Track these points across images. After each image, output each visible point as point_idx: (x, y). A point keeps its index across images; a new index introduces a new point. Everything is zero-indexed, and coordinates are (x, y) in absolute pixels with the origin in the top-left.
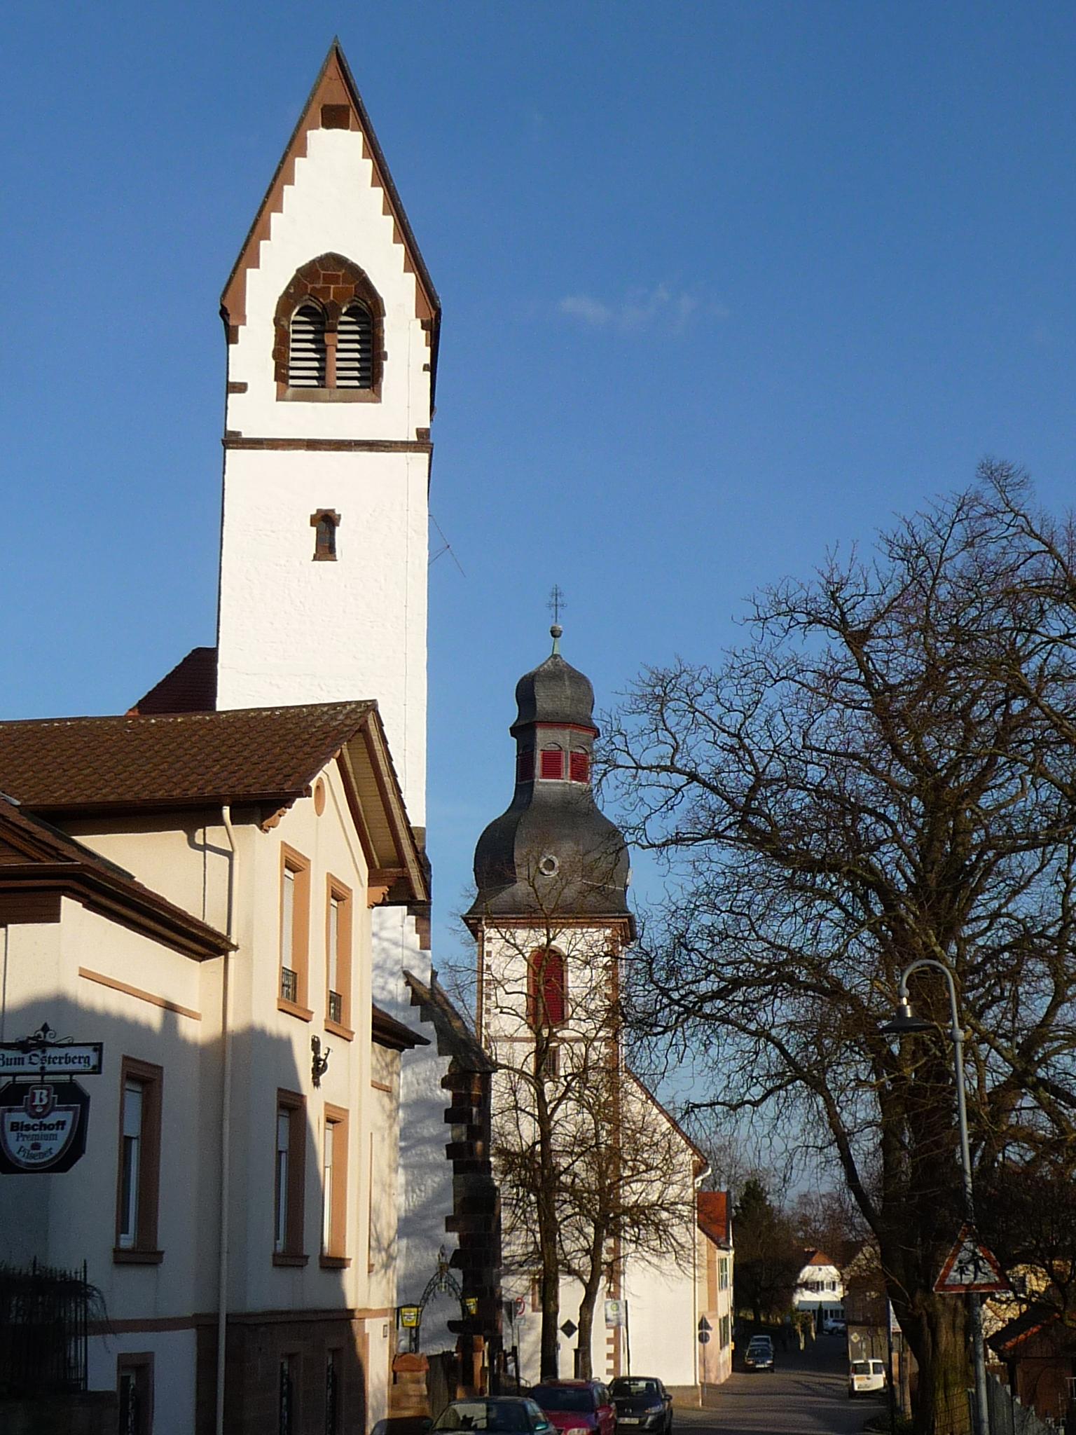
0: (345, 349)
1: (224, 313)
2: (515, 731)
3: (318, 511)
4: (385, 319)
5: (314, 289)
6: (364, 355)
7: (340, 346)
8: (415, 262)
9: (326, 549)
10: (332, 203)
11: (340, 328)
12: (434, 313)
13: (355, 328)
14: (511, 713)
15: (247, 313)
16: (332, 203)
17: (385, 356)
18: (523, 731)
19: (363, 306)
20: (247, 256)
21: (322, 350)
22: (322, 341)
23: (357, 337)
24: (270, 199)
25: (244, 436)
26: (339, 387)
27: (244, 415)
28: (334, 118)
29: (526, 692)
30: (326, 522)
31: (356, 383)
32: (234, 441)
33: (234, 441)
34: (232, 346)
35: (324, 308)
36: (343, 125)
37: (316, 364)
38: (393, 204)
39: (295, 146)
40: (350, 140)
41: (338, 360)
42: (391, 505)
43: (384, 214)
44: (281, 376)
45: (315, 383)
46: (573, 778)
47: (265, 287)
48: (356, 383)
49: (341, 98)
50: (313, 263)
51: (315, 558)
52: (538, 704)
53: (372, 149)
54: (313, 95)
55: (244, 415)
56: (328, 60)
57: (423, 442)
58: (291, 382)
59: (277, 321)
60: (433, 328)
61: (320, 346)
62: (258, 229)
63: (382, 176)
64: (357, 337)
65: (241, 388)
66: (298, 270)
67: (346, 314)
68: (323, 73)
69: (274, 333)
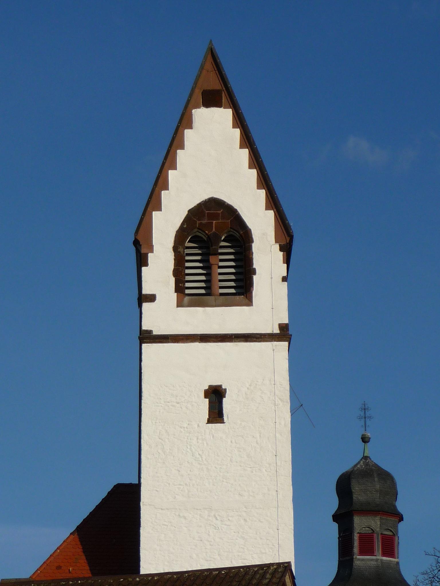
0: (224, 267)
1: (136, 243)
2: (336, 518)
3: (210, 386)
4: (253, 245)
5: (201, 224)
6: (239, 270)
7: (221, 264)
8: (273, 202)
9: (216, 415)
10: (212, 162)
11: (220, 251)
12: (288, 239)
13: (232, 250)
14: (333, 503)
15: (154, 244)
16: (212, 162)
17: (254, 272)
18: (343, 518)
19: (237, 235)
20: (153, 202)
21: (207, 267)
22: (208, 261)
23: (232, 257)
24: (169, 161)
25: (154, 333)
26: (222, 294)
27: (153, 318)
28: (211, 100)
29: (344, 486)
30: (215, 395)
31: (233, 291)
32: (147, 337)
33: (147, 337)
34: (144, 269)
35: (209, 237)
36: (218, 104)
37: (203, 278)
38: (256, 161)
39: (185, 121)
40: (224, 115)
41: (220, 274)
42: (260, 381)
43: (250, 168)
44: (180, 289)
45: (203, 291)
46: (384, 555)
47: (166, 225)
48: (233, 291)
49: (215, 84)
50: (200, 205)
51: (209, 421)
52: (355, 497)
53: (239, 121)
54: (196, 83)
55: (153, 318)
56: (205, 58)
57: (284, 333)
58: (187, 291)
59: (175, 249)
60: (287, 249)
61: (206, 264)
62: (160, 183)
63: (247, 141)
64: (232, 257)
65: (152, 298)
66: (189, 211)
67: (224, 241)
68: (202, 68)
69: (173, 257)
